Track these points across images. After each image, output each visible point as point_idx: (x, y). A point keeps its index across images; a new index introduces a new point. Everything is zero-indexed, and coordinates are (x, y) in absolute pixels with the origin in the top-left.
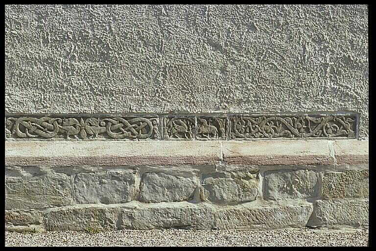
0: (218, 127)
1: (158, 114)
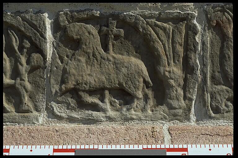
0: (152, 59)
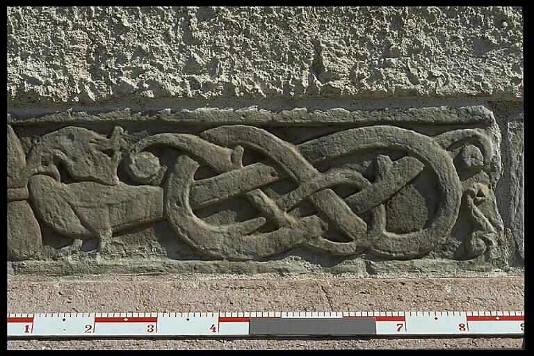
1: (491, 104)
